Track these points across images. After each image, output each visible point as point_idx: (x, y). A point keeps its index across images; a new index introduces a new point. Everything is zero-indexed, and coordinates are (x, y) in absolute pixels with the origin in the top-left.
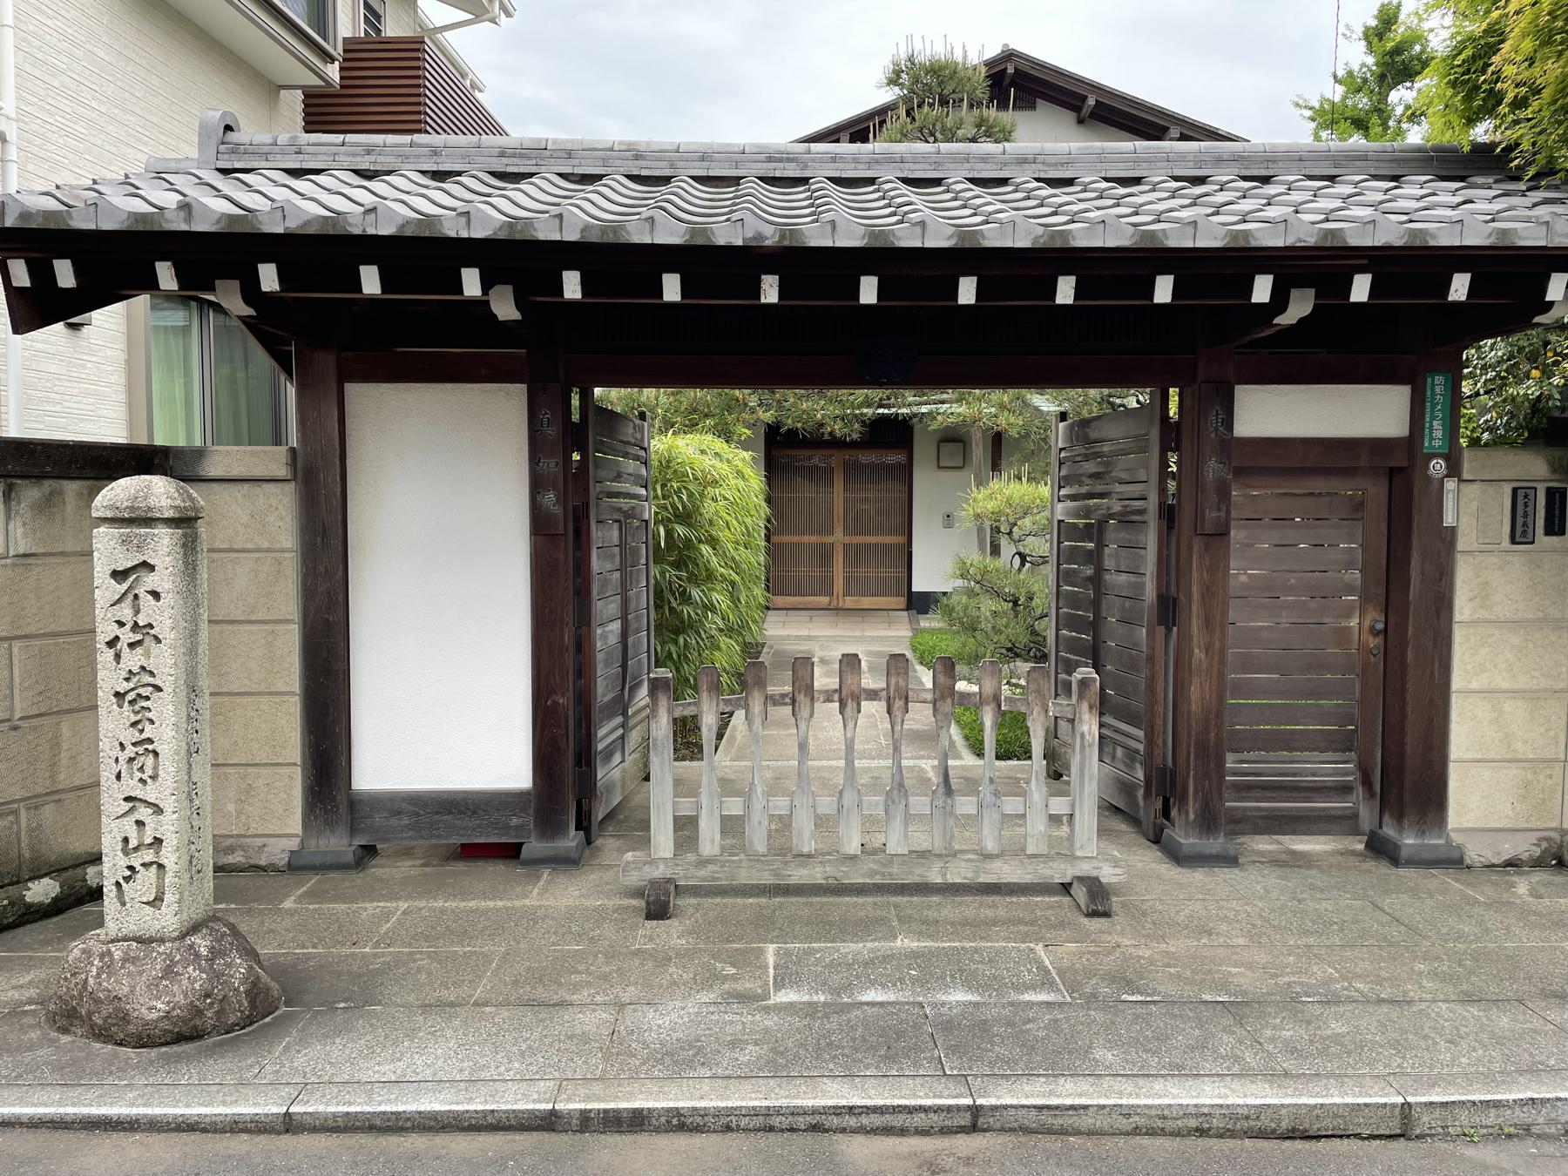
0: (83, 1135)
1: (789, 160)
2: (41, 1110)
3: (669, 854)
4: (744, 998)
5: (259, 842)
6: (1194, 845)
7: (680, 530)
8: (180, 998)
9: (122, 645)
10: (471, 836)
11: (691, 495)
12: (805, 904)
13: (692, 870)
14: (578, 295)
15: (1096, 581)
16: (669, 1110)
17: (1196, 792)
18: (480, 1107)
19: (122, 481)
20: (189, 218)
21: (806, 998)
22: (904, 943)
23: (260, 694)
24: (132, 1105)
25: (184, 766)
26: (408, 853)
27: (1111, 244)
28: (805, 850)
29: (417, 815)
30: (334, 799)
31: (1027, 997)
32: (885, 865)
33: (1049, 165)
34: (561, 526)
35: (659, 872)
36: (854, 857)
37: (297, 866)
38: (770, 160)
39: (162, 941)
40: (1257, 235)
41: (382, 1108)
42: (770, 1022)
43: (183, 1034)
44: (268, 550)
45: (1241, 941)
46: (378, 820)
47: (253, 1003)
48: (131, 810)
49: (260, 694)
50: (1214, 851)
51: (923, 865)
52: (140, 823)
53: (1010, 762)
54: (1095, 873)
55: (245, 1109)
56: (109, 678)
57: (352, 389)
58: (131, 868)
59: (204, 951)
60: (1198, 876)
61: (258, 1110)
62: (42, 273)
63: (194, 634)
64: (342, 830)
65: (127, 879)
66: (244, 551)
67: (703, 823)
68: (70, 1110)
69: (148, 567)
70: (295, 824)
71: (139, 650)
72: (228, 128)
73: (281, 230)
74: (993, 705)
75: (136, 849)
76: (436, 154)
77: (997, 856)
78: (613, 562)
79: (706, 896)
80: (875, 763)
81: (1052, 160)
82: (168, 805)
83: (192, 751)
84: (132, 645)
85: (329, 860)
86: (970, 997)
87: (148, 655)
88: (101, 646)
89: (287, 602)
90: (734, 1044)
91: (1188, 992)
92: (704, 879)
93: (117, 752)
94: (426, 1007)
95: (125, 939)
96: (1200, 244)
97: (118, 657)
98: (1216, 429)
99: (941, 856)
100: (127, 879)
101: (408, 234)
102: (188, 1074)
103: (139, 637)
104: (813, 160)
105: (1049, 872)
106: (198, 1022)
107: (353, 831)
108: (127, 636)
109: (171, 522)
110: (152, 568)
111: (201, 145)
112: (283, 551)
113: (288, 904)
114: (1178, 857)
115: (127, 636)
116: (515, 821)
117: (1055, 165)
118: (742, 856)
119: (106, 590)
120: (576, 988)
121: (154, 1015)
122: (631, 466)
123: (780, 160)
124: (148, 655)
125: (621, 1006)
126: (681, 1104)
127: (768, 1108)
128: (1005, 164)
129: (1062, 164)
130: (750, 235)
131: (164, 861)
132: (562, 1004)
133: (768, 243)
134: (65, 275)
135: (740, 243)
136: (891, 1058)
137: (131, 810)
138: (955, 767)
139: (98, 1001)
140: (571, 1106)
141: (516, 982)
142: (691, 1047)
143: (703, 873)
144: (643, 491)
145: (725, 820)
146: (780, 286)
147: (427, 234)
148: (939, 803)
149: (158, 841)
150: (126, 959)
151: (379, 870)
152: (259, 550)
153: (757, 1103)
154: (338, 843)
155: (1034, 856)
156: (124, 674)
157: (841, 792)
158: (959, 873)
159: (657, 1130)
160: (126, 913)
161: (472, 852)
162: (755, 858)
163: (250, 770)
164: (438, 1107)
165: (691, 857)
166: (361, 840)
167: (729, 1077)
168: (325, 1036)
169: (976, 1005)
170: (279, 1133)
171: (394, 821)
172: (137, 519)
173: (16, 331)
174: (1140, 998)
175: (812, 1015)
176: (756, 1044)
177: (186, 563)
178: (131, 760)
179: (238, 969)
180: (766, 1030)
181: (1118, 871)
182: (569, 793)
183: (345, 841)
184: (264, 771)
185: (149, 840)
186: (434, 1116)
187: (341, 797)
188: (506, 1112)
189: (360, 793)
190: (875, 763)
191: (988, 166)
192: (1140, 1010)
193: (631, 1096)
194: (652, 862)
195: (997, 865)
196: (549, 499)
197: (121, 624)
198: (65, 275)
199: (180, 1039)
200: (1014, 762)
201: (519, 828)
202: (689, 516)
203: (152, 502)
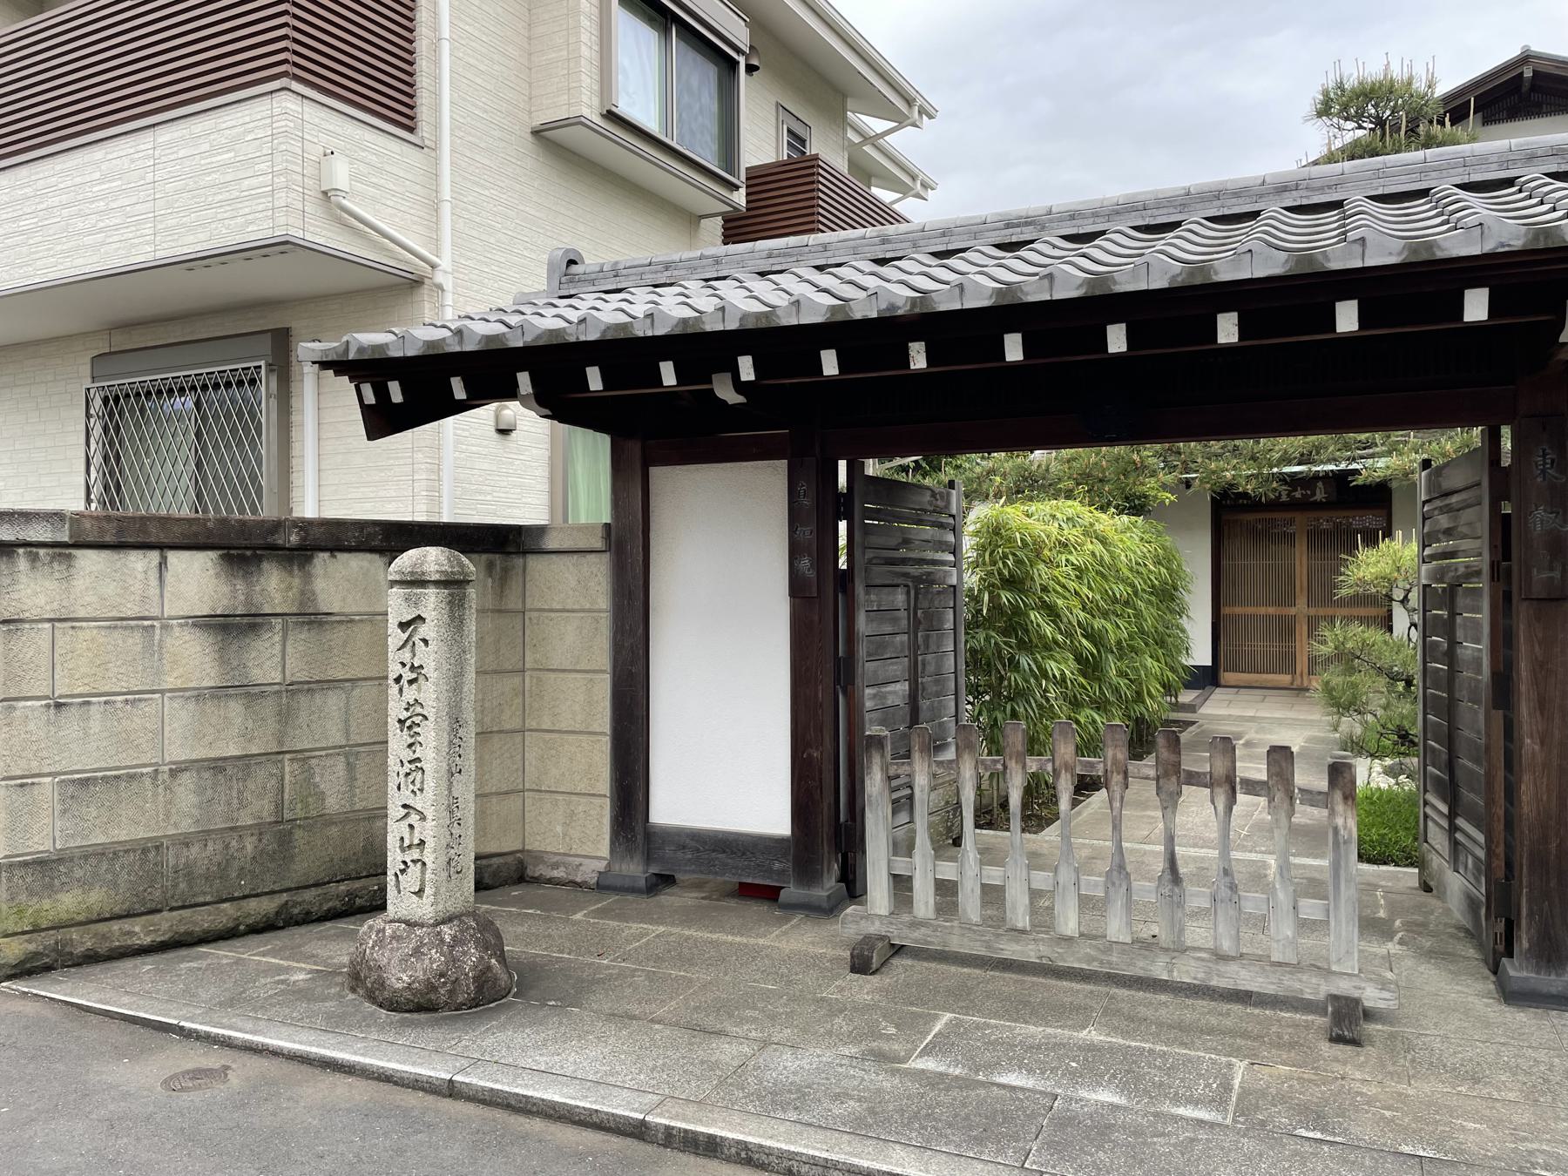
0: (317, 1071)
1: (1027, 224)
2: (297, 1046)
3: (884, 911)
4: (881, 1057)
5: (577, 861)
6: (1526, 979)
7: (1005, 597)
8: (420, 975)
9: (404, 681)
10: (747, 877)
11: (1019, 562)
12: (1016, 981)
13: (906, 931)
14: (836, 372)
15: (1450, 656)
16: (738, 1142)
17: (1531, 914)
18: (588, 1105)
19: (411, 552)
20: (461, 342)
21: (942, 1069)
22: (1091, 1035)
23: (581, 732)
24: (355, 1053)
25: (444, 784)
26: (698, 886)
27: (1259, 274)
28: (1020, 925)
29: (698, 850)
30: (633, 830)
31: (1181, 1111)
32: (1103, 952)
33: (1313, 189)
34: (815, 589)
35: (875, 928)
36: (1071, 939)
37: (604, 886)
38: (1008, 226)
39: (422, 926)
40: (1442, 243)
41: (517, 1090)
42: (887, 1083)
43: (420, 1006)
44: (589, 611)
45: (1511, 1096)
46: (668, 851)
47: (479, 989)
48: (406, 815)
49: (581, 732)
50: (1553, 990)
51: (1145, 957)
52: (411, 827)
53: (1384, 868)
54: (1356, 994)
55: (425, 1071)
56: (396, 710)
57: (656, 472)
58: (405, 863)
59: (448, 939)
60: (1522, 1018)
61: (432, 1074)
62: (382, 393)
63: (459, 675)
64: (638, 858)
65: (403, 871)
66: (573, 611)
67: (917, 884)
68: (314, 1050)
69: (420, 618)
70: (605, 851)
71: (414, 686)
72: (572, 262)
73: (521, 344)
74: (1227, 787)
75: (409, 847)
76: (717, 263)
77: (1233, 958)
78: (895, 620)
79: (926, 959)
80: (1203, 852)
81: (1317, 184)
82: (429, 814)
83: (453, 772)
84: (411, 682)
85: (627, 883)
86: (1116, 1100)
87: (419, 690)
88: (391, 682)
89: (600, 655)
90: (839, 1097)
91: (1388, 1140)
92: (916, 941)
93: (398, 768)
94: (612, 1016)
95: (399, 921)
96: (1370, 263)
97: (401, 690)
98: (1544, 471)
99: (1167, 950)
100: (403, 871)
101: (750, 326)
102: (408, 1037)
103: (414, 676)
104: (1051, 221)
105: (1297, 985)
106: (433, 997)
107: (648, 859)
108: (408, 675)
109: (437, 583)
110: (424, 620)
111: (549, 278)
112: (600, 611)
113: (578, 916)
114: (1513, 996)
115: (408, 675)
116: (777, 866)
117: (1322, 188)
118: (956, 923)
119: (396, 637)
120: (742, 1021)
121: (399, 985)
122: (928, 531)
123: (1018, 226)
124: (419, 690)
125: (765, 1044)
126: (750, 1139)
127: (826, 1160)
128: (1261, 196)
129: (1329, 187)
130: (883, 306)
131: (426, 860)
132: (720, 1033)
133: (900, 312)
134: (396, 393)
135: (874, 315)
136: (979, 1141)
137: (406, 815)
138: (1132, 851)
139: (370, 969)
140: (659, 1120)
141: (696, 1008)
142: (798, 1090)
143: (916, 934)
144: (951, 558)
145: (985, 888)
146: (927, 352)
147: (622, 336)
148: (1166, 891)
149: (422, 842)
150: (394, 937)
151: (669, 899)
152: (583, 611)
153: (817, 1154)
154: (634, 869)
155: (1280, 964)
156: (404, 705)
157: (1056, 868)
158: (1188, 971)
159: (728, 1160)
160: (408, 899)
161: (748, 892)
162: (967, 927)
163: (574, 798)
164: (557, 1098)
165: (906, 918)
166: (654, 869)
167: (810, 1125)
168: (522, 1025)
169: (1114, 1107)
170: (445, 1096)
171: (680, 854)
172: (416, 582)
173: (369, 439)
174: (1318, 1135)
175: (933, 1086)
176: (859, 1100)
177: (452, 617)
178: (407, 774)
179: (471, 956)
180: (879, 1091)
181: (1386, 995)
182: (824, 843)
183: (641, 868)
184: (583, 800)
185: (416, 841)
186: (553, 1105)
187: (639, 828)
188: (607, 1114)
189: (654, 826)
190: (1203, 852)
191: (1240, 201)
192: (1307, 1148)
193: (714, 1122)
194: (868, 917)
195: (1233, 968)
196: (805, 563)
197: (404, 665)
198: (396, 393)
199: (419, 1009)
200: (1391, 868)
201: (782, 872)
202: (1022, 582)
203: (426, 568)
